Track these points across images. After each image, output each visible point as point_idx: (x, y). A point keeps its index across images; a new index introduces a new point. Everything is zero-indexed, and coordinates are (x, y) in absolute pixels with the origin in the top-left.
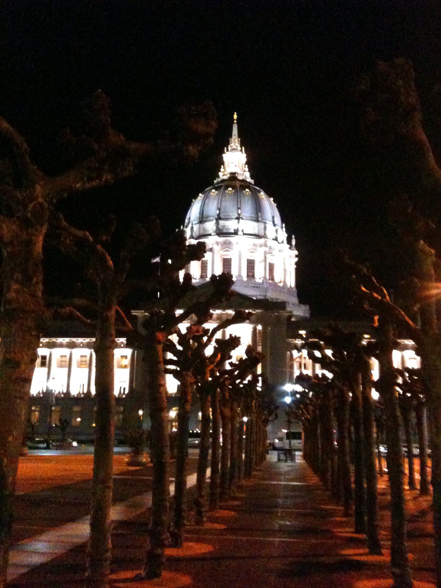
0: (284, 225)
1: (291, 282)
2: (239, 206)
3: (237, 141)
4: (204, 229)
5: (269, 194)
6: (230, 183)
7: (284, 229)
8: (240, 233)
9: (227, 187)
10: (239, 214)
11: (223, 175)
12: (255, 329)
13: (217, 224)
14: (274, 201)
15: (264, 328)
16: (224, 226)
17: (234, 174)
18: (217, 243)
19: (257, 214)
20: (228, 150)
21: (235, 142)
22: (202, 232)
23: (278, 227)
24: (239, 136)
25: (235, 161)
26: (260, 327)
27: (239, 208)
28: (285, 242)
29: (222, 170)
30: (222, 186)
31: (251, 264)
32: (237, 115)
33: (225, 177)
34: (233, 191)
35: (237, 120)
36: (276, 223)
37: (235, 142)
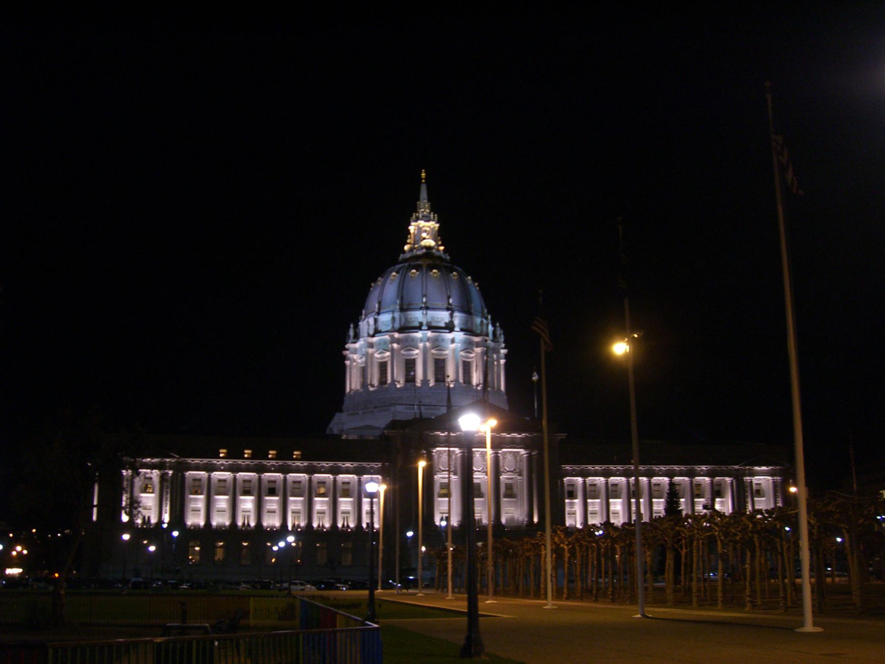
1: (503, 388)
4: (406, 319)
5: (474, 280)
6: (429, 262)
8: (457, 329)
9: (430, 268)
16: (433, 318)
17: (429, 248)
18: (428, 340)
21: (424, 208)
24: (429, 200)
25: (424, 230)
27: (449, 297)
31: (467, 366)
32: (425, 172)
33: (415, 252)
37: (424, 208)
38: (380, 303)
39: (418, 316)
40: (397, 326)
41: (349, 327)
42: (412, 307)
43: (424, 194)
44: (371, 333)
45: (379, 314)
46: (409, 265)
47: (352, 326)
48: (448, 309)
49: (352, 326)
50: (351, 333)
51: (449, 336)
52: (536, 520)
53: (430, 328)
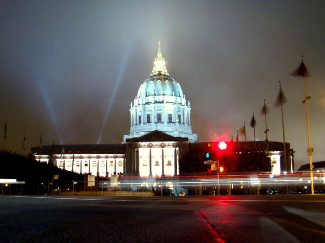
0: (184, 96)
2: (164, 89)
3: (160, 55)
7: (184, 98)
8: (165, 102)
9: (158, 79)
10: (164, 93)
11: (155, 72)
12: (176, 149)
13: (154, 97)
14: (179, 84)
15: (180, 149)
17: (160, 72)
19: (172, 92)
20: (156, 60)
21: (160, 55)
22: (147, 101)
23: (182, 97)
26: (177, 149)
27: (164, 90)
28: (185, 105)
29: (154, 69)
30: (155, 78)
34: (161, 81)
35: (160, 45)
36: (181, 95)
37: (160, 55)
38: (140, 94)
39: (151, 99)
40: (144, 103)
41: (131, 103)
42: (150, 95)
43: (159, 50)
44: (137, 105)
45: (139, 98)
46: (151, 79)
47: (132, 103)
48: (163, 95)
49: (132, 103)
50: (131, 105)
51: (164, 105)
52: (178, 174)
53: (156, 102)
